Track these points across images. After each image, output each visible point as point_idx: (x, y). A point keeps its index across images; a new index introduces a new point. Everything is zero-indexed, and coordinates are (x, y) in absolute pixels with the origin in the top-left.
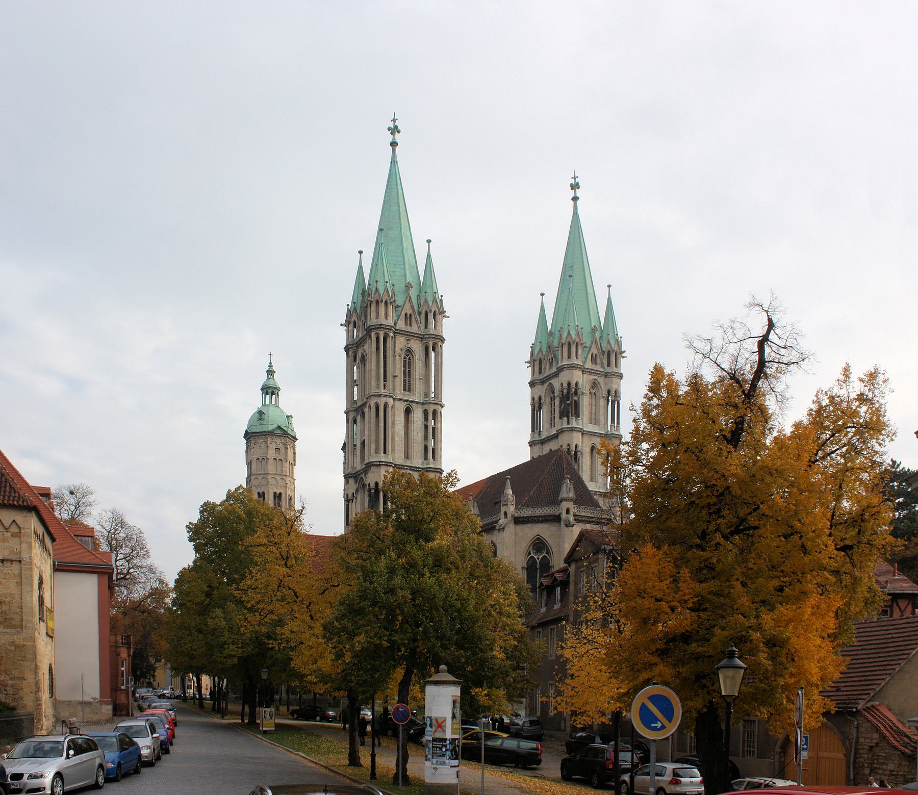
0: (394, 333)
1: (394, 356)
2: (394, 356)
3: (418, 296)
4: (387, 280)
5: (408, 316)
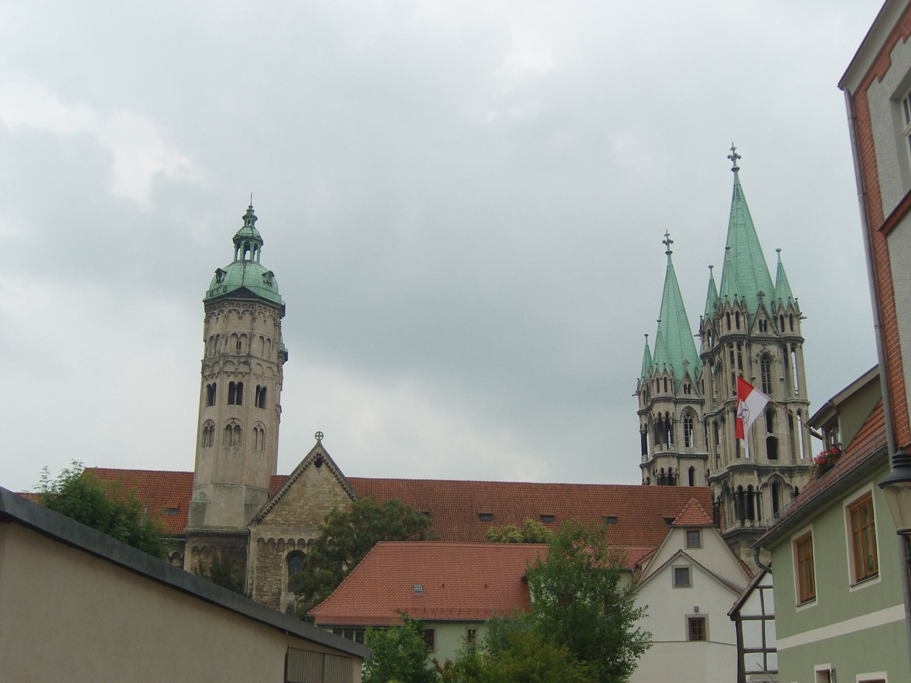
0: (749, 340)
1: (750, 362)
2: (750, 362)
3: (773, 303)
5: (763, 323)
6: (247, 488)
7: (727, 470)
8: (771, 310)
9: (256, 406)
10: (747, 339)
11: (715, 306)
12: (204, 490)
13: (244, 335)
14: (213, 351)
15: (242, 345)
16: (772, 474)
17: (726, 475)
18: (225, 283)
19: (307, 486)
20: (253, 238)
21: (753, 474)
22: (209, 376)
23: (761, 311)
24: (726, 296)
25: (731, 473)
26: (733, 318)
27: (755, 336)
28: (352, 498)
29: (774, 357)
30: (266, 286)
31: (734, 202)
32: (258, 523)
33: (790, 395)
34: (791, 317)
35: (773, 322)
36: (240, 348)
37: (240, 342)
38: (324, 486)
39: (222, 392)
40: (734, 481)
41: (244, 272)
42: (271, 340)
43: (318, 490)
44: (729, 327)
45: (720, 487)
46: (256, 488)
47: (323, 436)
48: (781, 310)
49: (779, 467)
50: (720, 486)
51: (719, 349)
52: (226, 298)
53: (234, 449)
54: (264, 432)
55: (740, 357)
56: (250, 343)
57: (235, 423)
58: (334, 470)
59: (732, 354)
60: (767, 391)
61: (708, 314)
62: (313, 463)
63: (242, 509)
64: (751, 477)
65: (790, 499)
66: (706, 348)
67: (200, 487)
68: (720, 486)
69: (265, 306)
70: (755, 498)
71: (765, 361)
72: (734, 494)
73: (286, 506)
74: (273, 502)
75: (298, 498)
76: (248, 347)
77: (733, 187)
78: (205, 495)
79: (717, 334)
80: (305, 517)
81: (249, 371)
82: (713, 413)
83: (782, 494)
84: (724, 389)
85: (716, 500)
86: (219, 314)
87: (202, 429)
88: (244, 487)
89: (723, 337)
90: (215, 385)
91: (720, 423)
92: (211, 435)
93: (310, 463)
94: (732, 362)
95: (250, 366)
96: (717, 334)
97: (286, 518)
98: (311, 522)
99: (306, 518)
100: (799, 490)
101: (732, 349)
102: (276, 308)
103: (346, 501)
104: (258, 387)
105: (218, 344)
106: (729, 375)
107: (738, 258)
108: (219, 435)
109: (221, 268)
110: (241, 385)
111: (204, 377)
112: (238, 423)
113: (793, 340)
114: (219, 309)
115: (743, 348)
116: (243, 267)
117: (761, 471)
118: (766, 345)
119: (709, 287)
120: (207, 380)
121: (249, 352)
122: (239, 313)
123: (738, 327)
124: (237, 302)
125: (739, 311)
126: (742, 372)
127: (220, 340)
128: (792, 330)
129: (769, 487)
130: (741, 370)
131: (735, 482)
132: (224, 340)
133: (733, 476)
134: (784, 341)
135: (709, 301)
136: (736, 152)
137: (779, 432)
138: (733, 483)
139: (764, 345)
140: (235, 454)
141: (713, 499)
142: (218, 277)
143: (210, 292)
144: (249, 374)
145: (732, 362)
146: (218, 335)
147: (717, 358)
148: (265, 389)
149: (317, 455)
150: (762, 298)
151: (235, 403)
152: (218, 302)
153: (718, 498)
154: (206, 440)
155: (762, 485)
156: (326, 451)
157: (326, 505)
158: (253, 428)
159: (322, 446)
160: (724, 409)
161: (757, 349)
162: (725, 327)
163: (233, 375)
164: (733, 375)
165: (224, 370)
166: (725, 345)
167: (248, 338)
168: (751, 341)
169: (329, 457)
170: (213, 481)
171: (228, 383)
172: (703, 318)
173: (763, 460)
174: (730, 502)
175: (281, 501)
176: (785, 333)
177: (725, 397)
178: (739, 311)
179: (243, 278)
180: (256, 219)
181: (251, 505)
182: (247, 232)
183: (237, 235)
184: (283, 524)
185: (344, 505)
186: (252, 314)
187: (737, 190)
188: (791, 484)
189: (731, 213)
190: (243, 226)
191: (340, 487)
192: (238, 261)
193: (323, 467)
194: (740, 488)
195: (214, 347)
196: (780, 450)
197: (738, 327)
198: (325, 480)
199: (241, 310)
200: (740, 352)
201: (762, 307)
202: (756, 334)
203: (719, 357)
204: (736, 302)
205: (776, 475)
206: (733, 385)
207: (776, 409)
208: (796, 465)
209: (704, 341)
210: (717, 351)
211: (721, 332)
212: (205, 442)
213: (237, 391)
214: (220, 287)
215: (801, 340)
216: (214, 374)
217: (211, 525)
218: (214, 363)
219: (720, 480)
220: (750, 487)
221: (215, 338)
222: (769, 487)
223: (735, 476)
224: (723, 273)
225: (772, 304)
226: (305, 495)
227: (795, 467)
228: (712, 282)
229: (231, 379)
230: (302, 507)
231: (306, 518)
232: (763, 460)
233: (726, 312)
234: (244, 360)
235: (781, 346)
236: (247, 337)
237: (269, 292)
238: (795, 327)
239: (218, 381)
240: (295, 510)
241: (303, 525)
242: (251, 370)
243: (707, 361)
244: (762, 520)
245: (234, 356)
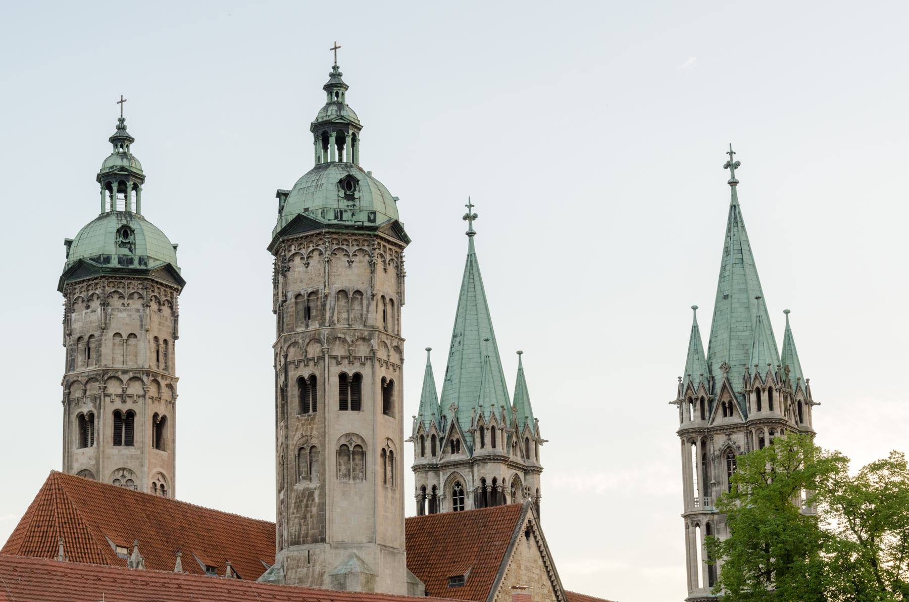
124: (354, 238)
238: (805, 417)
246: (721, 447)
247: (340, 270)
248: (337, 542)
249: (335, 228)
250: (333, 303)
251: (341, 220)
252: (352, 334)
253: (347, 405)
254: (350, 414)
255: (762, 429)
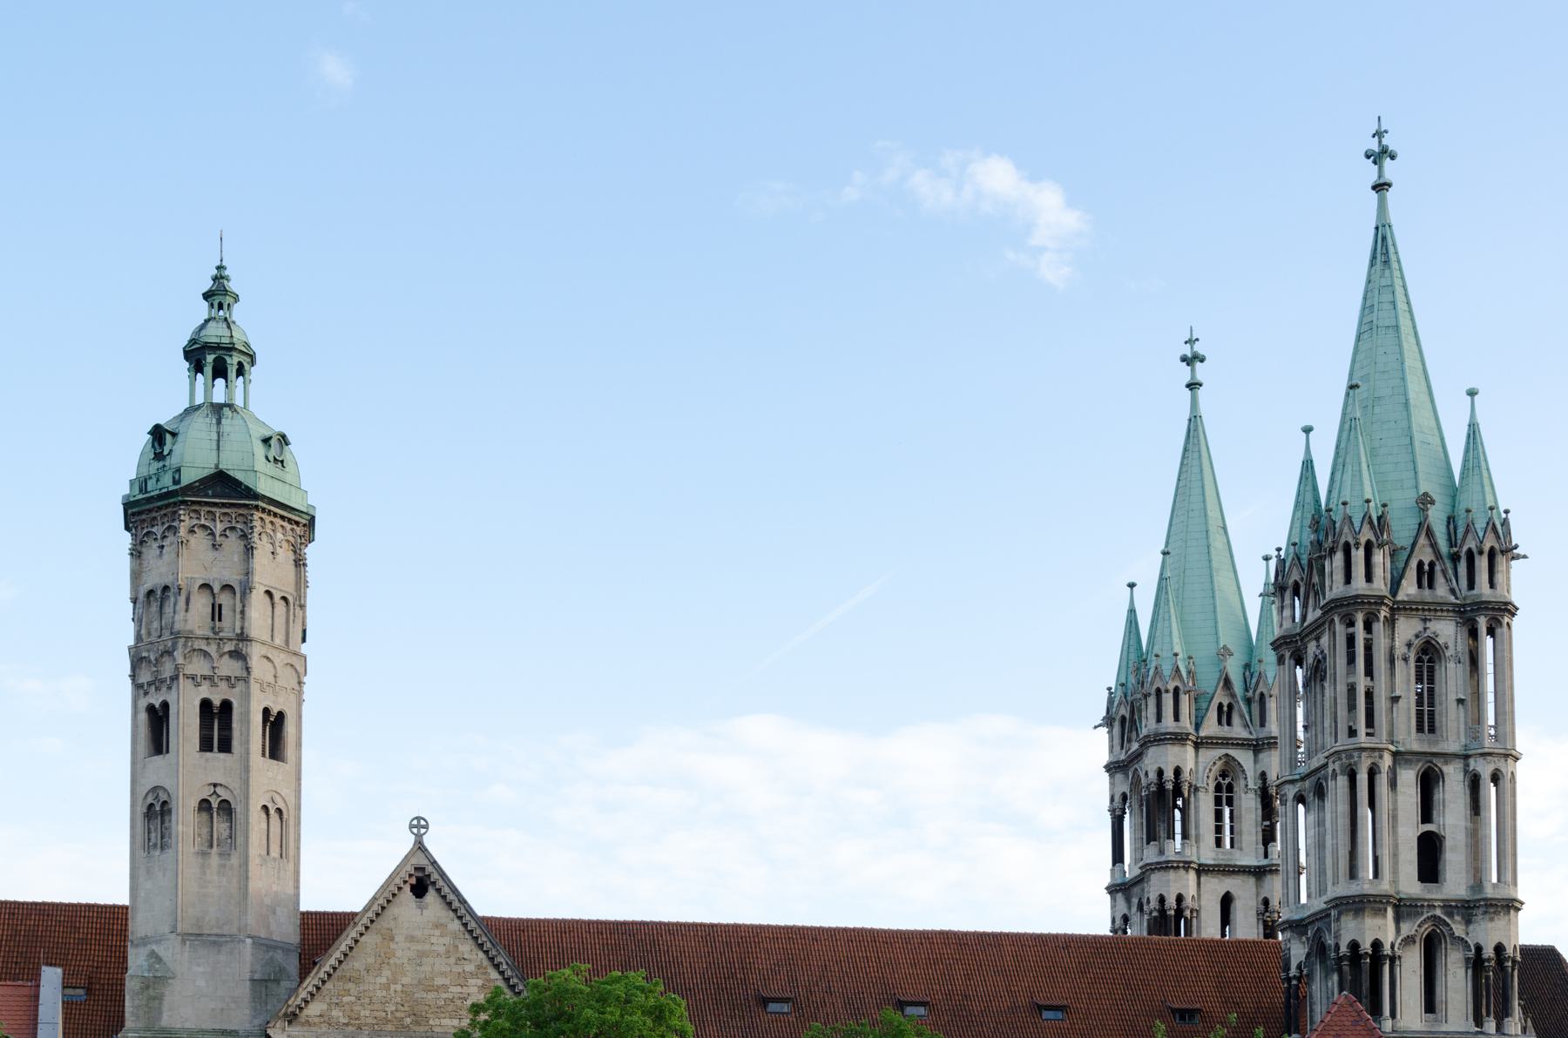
0: (1392, 609)
1: (1392, 661)
2: (1392, 661)
3: (1451, 520)
4: (1368, 496)
5: (1426, 568)
6: (254, 943)
7: (1324, 906)
8: (1446, 537)
9: (264, 755)
10: (1388, 606)
11: (1316, 524)
12: (154, 947)
13: (227, 587)
14: (156, 625)
15: (223, 612)
16: (1425, 916)
17: (1322, 916)
18: (173, 461)
19: (396, 939)
20: (231, 349)
21: (1385, 916)
22: (149, 684)
23: (1423, 540)
24: (1345, 504)
25: (1333, 913)
26: (1358, 556)
27: (1406, 599)
28: (497, 966)
29: (1447, 648)
30: (271, 469)
31: (1374, 268)
32: (290, 1022)
33: (1475, 738)
34: (1492, 555)
35: (1449, 565)
36: (220, 620)
37: (220, 606)
38: (433, 940)
39: (186, 725)
40: (1338, 930)
41: (218, 433)
42: (290, 599)
43: (419, 947)
44: (1348, 579)
45: (1304, 943)
46: (273, 943)
47: (426, 827)
48: (1470, 536)
49: (1442, 900)
50: (1304, 939)
51: (1319, 626)
52: (180, 498)
53: (220, 855)
54: (285, 816)
55: (1368, 648)
56: (244, 606)
57: (219, 796)
58: (456, 904)
59: (1351, 640)
60: (1426, 728)
61: (1294, 544)
62: (407, 888)
63: (245, 990)
64: (1378, 921)
65: (1463, 970)
66: (1287, 624)
67: (145, 941)
68: (1304, 939)
69: (272, 518)
70: (1386, 968)
71: (1426, 658)
72: (1340, 959)
73: (351, 985)
74: (321, 975)
75: (377, 966)
76: (238, 616)
77: (1373, 231)
78: (159, 960)
79: (1316, 593)
80: (394, 1008)
81: (245, 675)
82: (1297, 777)
83: (1446, 959)
84: (1327, 723)
85: (1293, 972)
86: (164, 537)
87: (141, 809)
88: (249, 941)
89: (1332, 601)
90: (165, 705)
91: (1312, 798)
92: (163, 822)
93: (400, 889)
94: (1351, 660)
95: (247, 663)
96: (1316, 593)
97: (352, 1011)
98: (408, 1020)
99: (397, 1011)
100: (1484, 951)
101: (1351, 630)
102: (297, 523)
103: (485, 973)
104: (266, 711)
105: (168, 609)
106: (1342, 689)
107: (1377, 410)
108: (185, 821)
109: (162, 422)
110: (227, 706)
111: (137, 685)
112: (224, 795)
113: (1493, 609)
114: (163, 523)
115: (1379, 627)
116: (214, 421)
117: (1404, 908)
118: (1430, 620)
119: (1301, 479)
120: (146, 693)
121: (242, 628)
122: (212, 534)
123: (1369, 577)
125: (1374, 539)
126: (1371, 684)
127: (172, 599)
128: (1492, 585)
129: (1418, 944)
130: (1369, 678)
131: (1342, 932)
132: (182, 599)
133: (1338, 919)
134: (1472, 610)
135: (1299, 514)
136: (1385, 142)
137: (1447, 822)
138: (1337, 936)
139: (1425, 620)
140: (224, 866)
141: (1287, 968)
142: (156, 445)
143: (142, 483)
144: (246, 680)
145: (1351, 660)
146: (166, 588)
147: (1312, 648)
148: (281, 715)
149: (415, 868)
150: (1428, 509)
151: (216, 749)
152: (160, 508)
153: (1299, 967)
154: (153, 835)
155: (1402, 940)
156: (435, 862)
157: (439, 981)
158: (259, 808)
159: (426, 850)
160: (1325, 766)
161: (1407, 628)
162: (1339, 576)
163: (207, 682)
164: (1352, 690)
165: (186, 672)
166: (1337, 619)
167: (238, 595)
168: (1398, 609)
169: (443, 875)
170: (175, 927)
171: (197, 703)
172: (1282, 553)
173: (1410, 884)
174: (1327, 976)
175: (338, 973)
176: (1475, 592)
177: (1329, 740)
178: (1374, 539)
179: (218, 449)
180: (236, 298)
181: (266, 981)
182: (215, 333)
183: (193, 341)
184: (347, 1025)
185: (480, 982)
186: (244, 536)
187: (1384, 238)
188: (1467, 939)
189: (1365, 298)
190: (206, 317)
191: (471, 942)
192: (199, 407)
193: (431, 896)
194: (1354, 946)
195: (157, 616)
196: (1447, 863)
197: (1369, 577)
198: (436, 927)
199: (219, 527)
200: (1369, 636)
201: (1425, 529)
202: (1408, 595)
203: (1318, 646)
204: (1367, 518)
205: (1434, 917)
206: (1349, 711)
207: (1445, 769)
208: (1479, 897)
209: (1282, 607)
210: (1314, 631)
211: (1327, 589)
212: (149, 839)
213: (219, 719)
214: (165, 472)
215: (1508, 609)
216: (162, 681)
217: (179, 1026)
218: (162, 656)
219: (1306, 926)
220: (1377, 945)
221: (159, 592)
222: (1418, 944)
223: (1343, 918)
224: (1338, 447)
225: (1449, 523)
226: (392, 961)
227: (1479, 900)
228: (1308, 466)
229: (205, 691)
230: (387, 987)
231: (397, 1011)
232: (1410, 884)
233: (1342, 541)
234: (233, 649)
235: (1464, 624)
236: (235, 594)
237: (281, 483)
238: (1499, 578)
239: (171, 698)
240: (371, 994)
241: (390, 1027)
242: (249, 673)
243: (1287, 655)
244: (1398, 1016)
245: (207, 639)
246: (1263, 667)
247: (151, 562)
248: (142, 938)
249: (137, 506)
250: (141, 610)
251: (146, 492)
252: (155, 649)
253: (213, 744)
254: (217, 757)
255: (1351, 614)
